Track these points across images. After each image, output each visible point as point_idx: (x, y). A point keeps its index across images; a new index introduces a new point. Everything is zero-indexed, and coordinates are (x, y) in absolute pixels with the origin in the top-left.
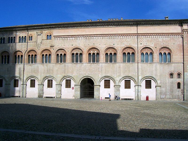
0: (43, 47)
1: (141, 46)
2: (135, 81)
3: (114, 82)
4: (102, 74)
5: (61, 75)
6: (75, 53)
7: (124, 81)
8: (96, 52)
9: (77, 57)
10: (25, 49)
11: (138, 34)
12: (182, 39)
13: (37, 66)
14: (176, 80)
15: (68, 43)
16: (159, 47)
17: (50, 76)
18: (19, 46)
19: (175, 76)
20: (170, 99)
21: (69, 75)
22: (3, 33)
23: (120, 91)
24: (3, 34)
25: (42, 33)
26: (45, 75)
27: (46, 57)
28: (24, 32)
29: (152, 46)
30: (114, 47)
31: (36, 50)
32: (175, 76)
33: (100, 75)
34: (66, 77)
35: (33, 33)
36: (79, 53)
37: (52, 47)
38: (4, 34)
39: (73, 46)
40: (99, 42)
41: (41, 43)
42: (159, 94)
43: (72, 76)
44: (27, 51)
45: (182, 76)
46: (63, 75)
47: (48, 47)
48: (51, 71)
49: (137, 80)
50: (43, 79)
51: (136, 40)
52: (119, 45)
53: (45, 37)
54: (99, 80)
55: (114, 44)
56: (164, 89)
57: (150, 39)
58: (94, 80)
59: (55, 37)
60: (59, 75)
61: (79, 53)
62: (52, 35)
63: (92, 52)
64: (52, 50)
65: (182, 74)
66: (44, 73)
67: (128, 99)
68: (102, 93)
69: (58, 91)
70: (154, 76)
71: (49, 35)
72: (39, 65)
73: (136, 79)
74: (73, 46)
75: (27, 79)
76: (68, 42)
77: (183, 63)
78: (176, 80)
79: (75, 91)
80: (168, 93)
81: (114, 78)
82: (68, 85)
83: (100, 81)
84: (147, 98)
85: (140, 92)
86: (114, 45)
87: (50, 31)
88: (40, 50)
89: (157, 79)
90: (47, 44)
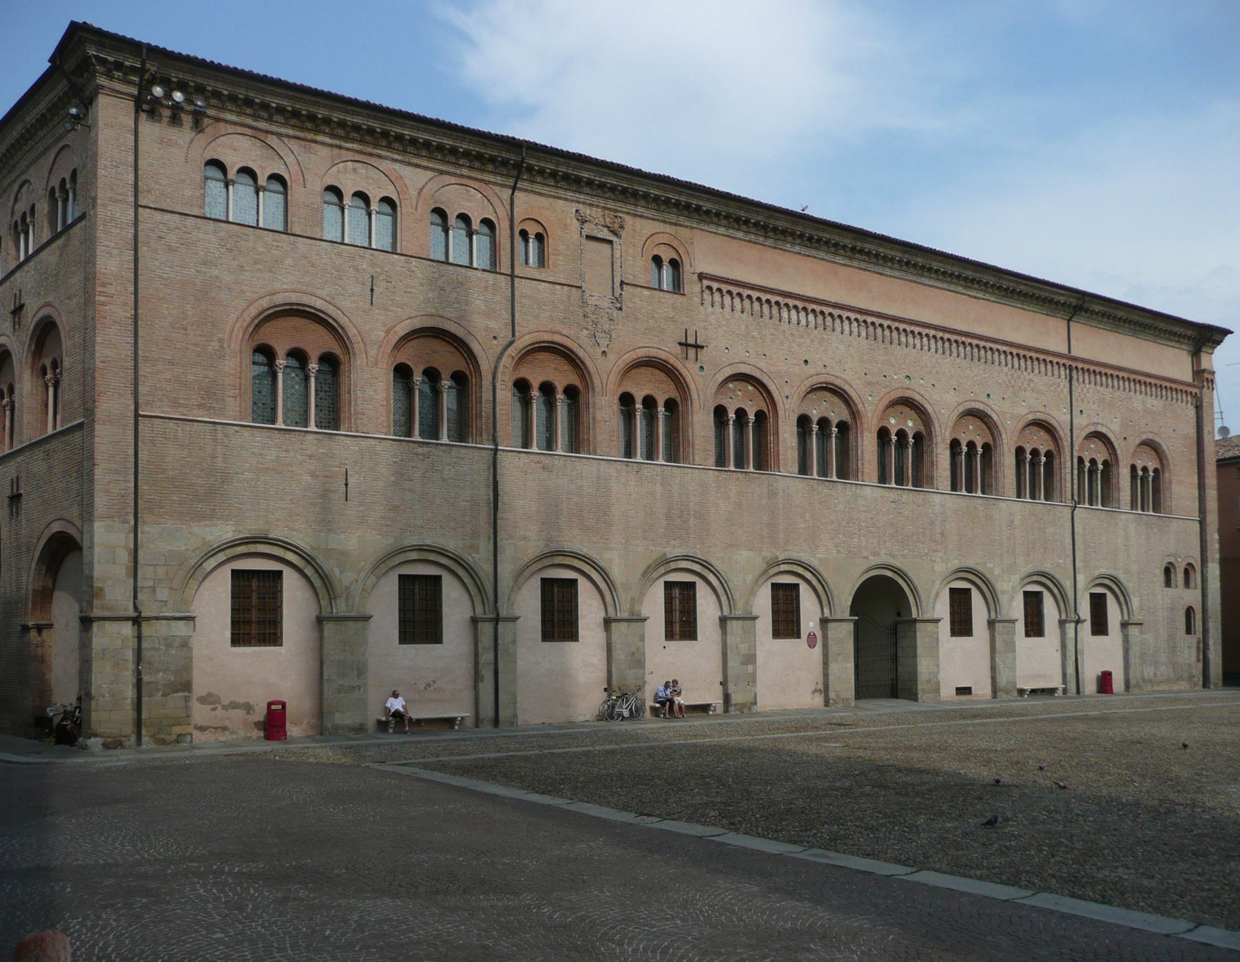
0: (634, 339)
1: (1083, 424)
2: (1061, 598)
3: (992, 599)
5: (752, 554)
6: (815, 415)
7: (1020, 598)
9: (830, 442)
11: (1075, 359)
13: (598, 478)
15: (782, 343)
17: (686, 558)
18: (443, 289)
19: (1179, 577)
20: (1168, 681)
21: (795, 555)
24: (258, 135)
26: (657, 551)
27: (656, 419)
28: (472, 183)
29: (1113, 429)
30: (989, 412)
31: (581, 353)
33: (938, 560)
34: (776, 570)
35: (558, 211)
36: (835, 419)
38: (273, 141)
39: (810, 369)
40: (930, 372)
42: (1137, 661)
43: (814, 562)
45: (1197, 578)
47: (668, 350)
48: (692, 521)
49: (1070, 593)
52: (1017, 397)
53: (638, 268)
54: (934, 592)
57: (1107, 392)
58: (914, 591)
59: (706, 283)
60: (743, 556)
61: (835, 419)
63: (893, 421)
64: (689, 371)
65: (1198, 567)
66: (645, 531)
67: (1043, 690)
68: (952, 664)
70: (1122, 577)
71: (666, 255)
72: (611, 470)
73: (1068, 585)
74: (810, 369)
75: (520, 576)
76: (781, 336)
77: (1201, 522)
80: (1163, 657)
81: (992, 580)
82: (786, 622)
84: (1105, 682)
88: (612, 357)
89: (1130, 586)
90: (651, 324)
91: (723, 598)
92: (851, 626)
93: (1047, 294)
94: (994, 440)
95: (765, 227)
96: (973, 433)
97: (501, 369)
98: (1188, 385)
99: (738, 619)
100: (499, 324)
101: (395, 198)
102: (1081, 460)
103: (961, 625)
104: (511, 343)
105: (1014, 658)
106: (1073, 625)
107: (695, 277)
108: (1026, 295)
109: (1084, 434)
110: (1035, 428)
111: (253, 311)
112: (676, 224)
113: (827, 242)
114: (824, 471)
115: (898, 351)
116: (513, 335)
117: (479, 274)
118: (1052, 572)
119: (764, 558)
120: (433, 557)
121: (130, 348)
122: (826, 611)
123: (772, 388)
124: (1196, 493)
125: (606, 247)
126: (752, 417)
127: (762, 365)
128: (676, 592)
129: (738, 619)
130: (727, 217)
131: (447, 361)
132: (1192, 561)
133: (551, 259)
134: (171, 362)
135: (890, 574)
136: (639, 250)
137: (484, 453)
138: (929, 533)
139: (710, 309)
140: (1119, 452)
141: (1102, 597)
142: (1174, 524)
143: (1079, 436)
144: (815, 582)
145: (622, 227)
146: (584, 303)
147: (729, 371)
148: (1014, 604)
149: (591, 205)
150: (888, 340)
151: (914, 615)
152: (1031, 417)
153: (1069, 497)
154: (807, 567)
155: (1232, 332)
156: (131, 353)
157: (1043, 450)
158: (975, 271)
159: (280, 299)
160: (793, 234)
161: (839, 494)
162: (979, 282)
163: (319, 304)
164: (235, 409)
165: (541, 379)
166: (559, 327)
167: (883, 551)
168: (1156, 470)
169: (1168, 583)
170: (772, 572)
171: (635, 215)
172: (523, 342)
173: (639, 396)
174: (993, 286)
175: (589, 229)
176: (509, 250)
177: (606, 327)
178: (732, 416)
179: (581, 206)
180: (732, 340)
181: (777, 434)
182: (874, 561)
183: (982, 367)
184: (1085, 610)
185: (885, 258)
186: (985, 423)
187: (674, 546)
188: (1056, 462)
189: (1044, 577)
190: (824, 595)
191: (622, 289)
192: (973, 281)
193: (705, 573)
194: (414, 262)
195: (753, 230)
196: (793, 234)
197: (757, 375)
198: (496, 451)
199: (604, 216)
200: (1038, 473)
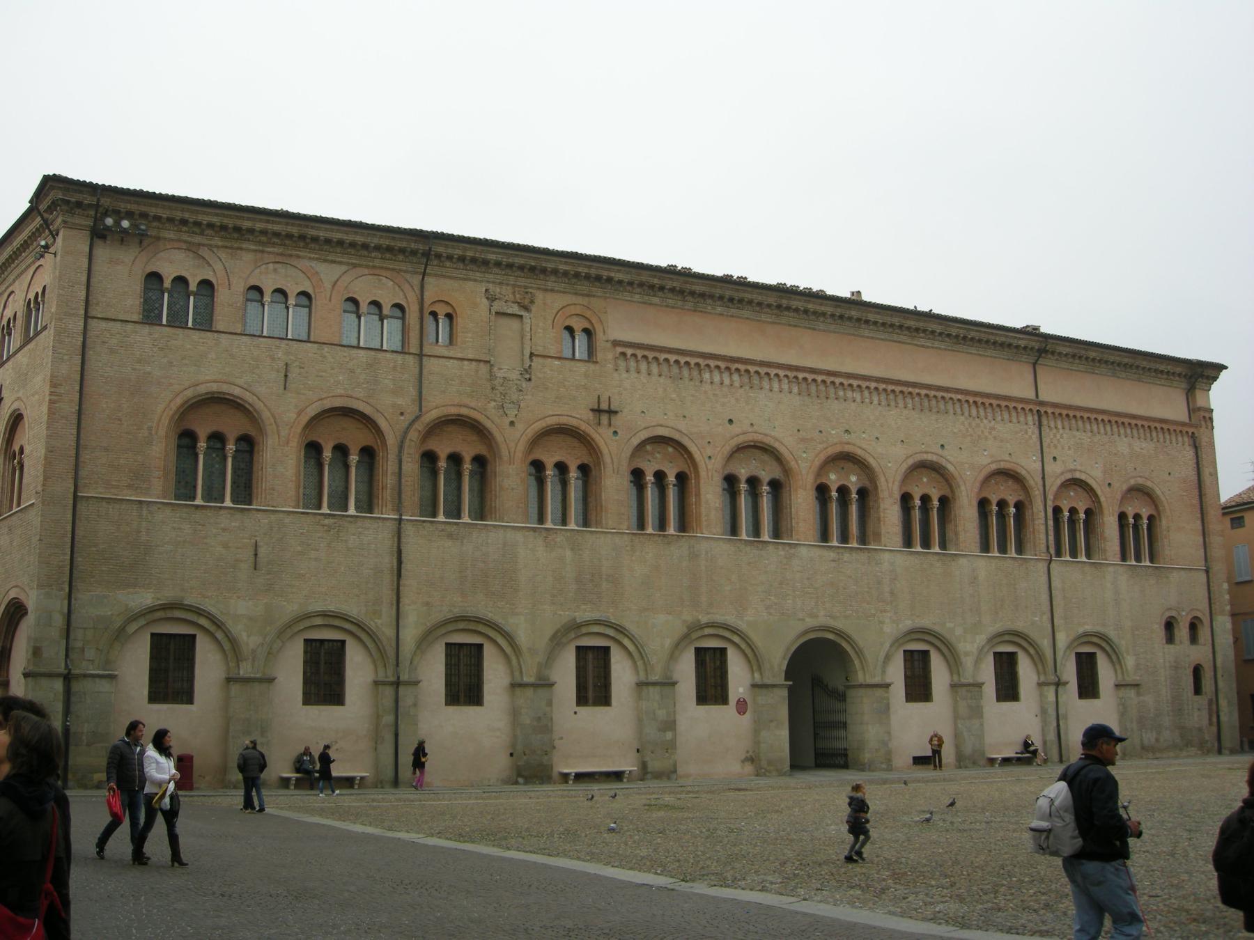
1: (1057, 472)
2: (1038, 659)
3: (953, 661)
4: (896, 613)
5: (670, 617)
6: (743, 473)
8: (853, 481)
10: (400, 401)
11: (1042, 404)
12: (1189, 453)
14: (1189, 653)
16: (1120, 487)
17: (597, 622)
18: (352, 371)
19: (1182, 632)
21: (719, 618)
22: (197, 239)
23: (981, 717)
25: (526, 302)
26: (566, 615)
29: (1094, 474)
30: (943, 462)
31: (488, 424)
32: (1182, 632)
33: (887, 621)
34: (700, 633)
36: (765, 476)
37: (605, 419)
41: (527, 374)
43: (743, 626)
44: (418, 418)
45: (1204, 633)
46: (688, 616)
47: (579, 416)
49: (1048, 653)
50: (554, 636)
51: (1035, 437)
55: (942, 446)
56: (1149, 699)
58: (859, 653)
59: (619, 349)
61: (765, 476)
62: (600, 336)
63: (833, 477)
64: (602, 437)
69: (659, 730)
70: (1112, 634)
72: (519, 537)
73: (1045, 644)
74: (735, 429)
75: (425, 640)
77: (1207, 572)
78: (1189, 653)
79: (758, 726)
80: (1167, 721)
83: (888, 658)
85: (1066, 718)
86: (945, 453)
87: (580, 300)
88: (520, 426)
89: (1123, 643)
90: (562, 393)
91: (640, 663)
92: (785, 693)
93: (1003, 339)
94: (953, 492)
95: (682, 292)
96: (924, 486)
97: (407, 443)
98: (1183, 424)
99: (654, 684)
100: (406, 401)
101: (310, 291)
102: (1057, 510)
103: (919, 688)
104: (418, 418)
105: (982, 725)
106: (1052, 689)
107: (609, 345)
108: (980, 341)
109: (1059, 482)
110: (999, 478)
111: (179, 401)
112: (588, 296)
113: (750, 302)
114: (844, 538)
115: (835, 406)
116: (421, 410)
117: (388, 355)
118: (1026, 631)
119: (684, 621)
120: (337, 622)
121: (74, 438)
122: (757, 675)
123: (693, 449)
124: (1201, 539)
125: (515, 324)
126: (671, 478)
127: (682, 426)
128: (590, 656)
129: (654, 684)
130: (641, 285)
131: (356, 439)
132: (1199, 615)
133: (460, 336)
134: (106, 449)
135: (831, 636)
136: (550, 322)
137: (388, 523)
138: (875, 593)
139: (625, 375)
140: (1102, 499)
141: (1091, 656)
142: (1174, 576)
143: (1053, 485)
144: (743, 646)
145: (532, 302)
146: (492, 376)
147: (644, 435)
148: (983, 666)
149: (501, 284)
150: (823, 395)
151: (861, 678)
152: (994, 467)
153: (1043, 547)
154: (735, 631)
155: (1226, 368)
156: (74, 444)
157: (1012, 500)
158: (918, 321)
159: (202, 389)
160: (712, 297)
161: (772, 556)
162: (925, 331)
163: (237, 391)
164: (157, 490)
165: (448, 450)
166: (466, 401)
167: (822, 613)
168: (1151, 518)
169: (1170, 639)
170: (694, 636)
171: (546, 290)
172: (431, 415)
173: (549, 461)
174: (940, 334)
175: (497, 306)
176: (417, 332)
177: (514, 398)
178: (650, 478)
179: (491, 286)
180: (649, 404)
181: (698, 495)
182: (810, 622)
183: (934, 417)
184: (1070, 672)
185: (815, 313)
186: (942, 475)
187: (585, 610)
188: (1028, 514)
189: (1015, 636)
190: (754, 659)
191: (531, 360)
192: (917, 330)
193: (619, 637)
194: (326, 348)
195: (670, 295)
196: (712, 297)
197: (677, 436)
198: (400, 520)
199: (514, 293)
200: (1004, 522)
